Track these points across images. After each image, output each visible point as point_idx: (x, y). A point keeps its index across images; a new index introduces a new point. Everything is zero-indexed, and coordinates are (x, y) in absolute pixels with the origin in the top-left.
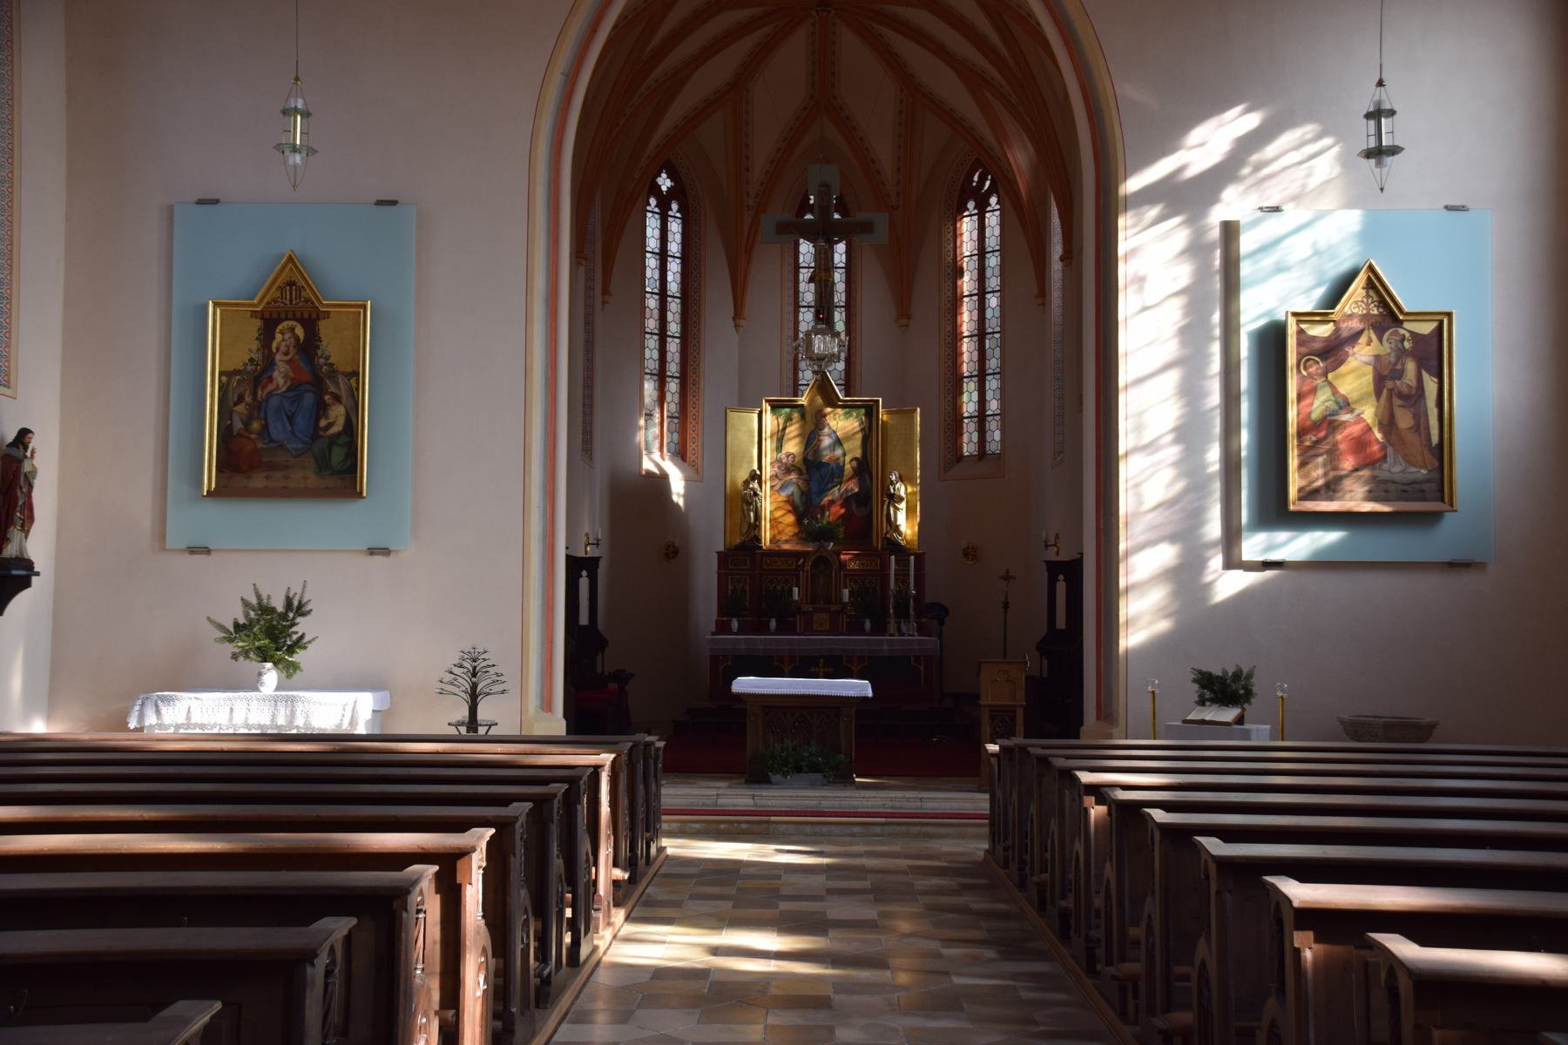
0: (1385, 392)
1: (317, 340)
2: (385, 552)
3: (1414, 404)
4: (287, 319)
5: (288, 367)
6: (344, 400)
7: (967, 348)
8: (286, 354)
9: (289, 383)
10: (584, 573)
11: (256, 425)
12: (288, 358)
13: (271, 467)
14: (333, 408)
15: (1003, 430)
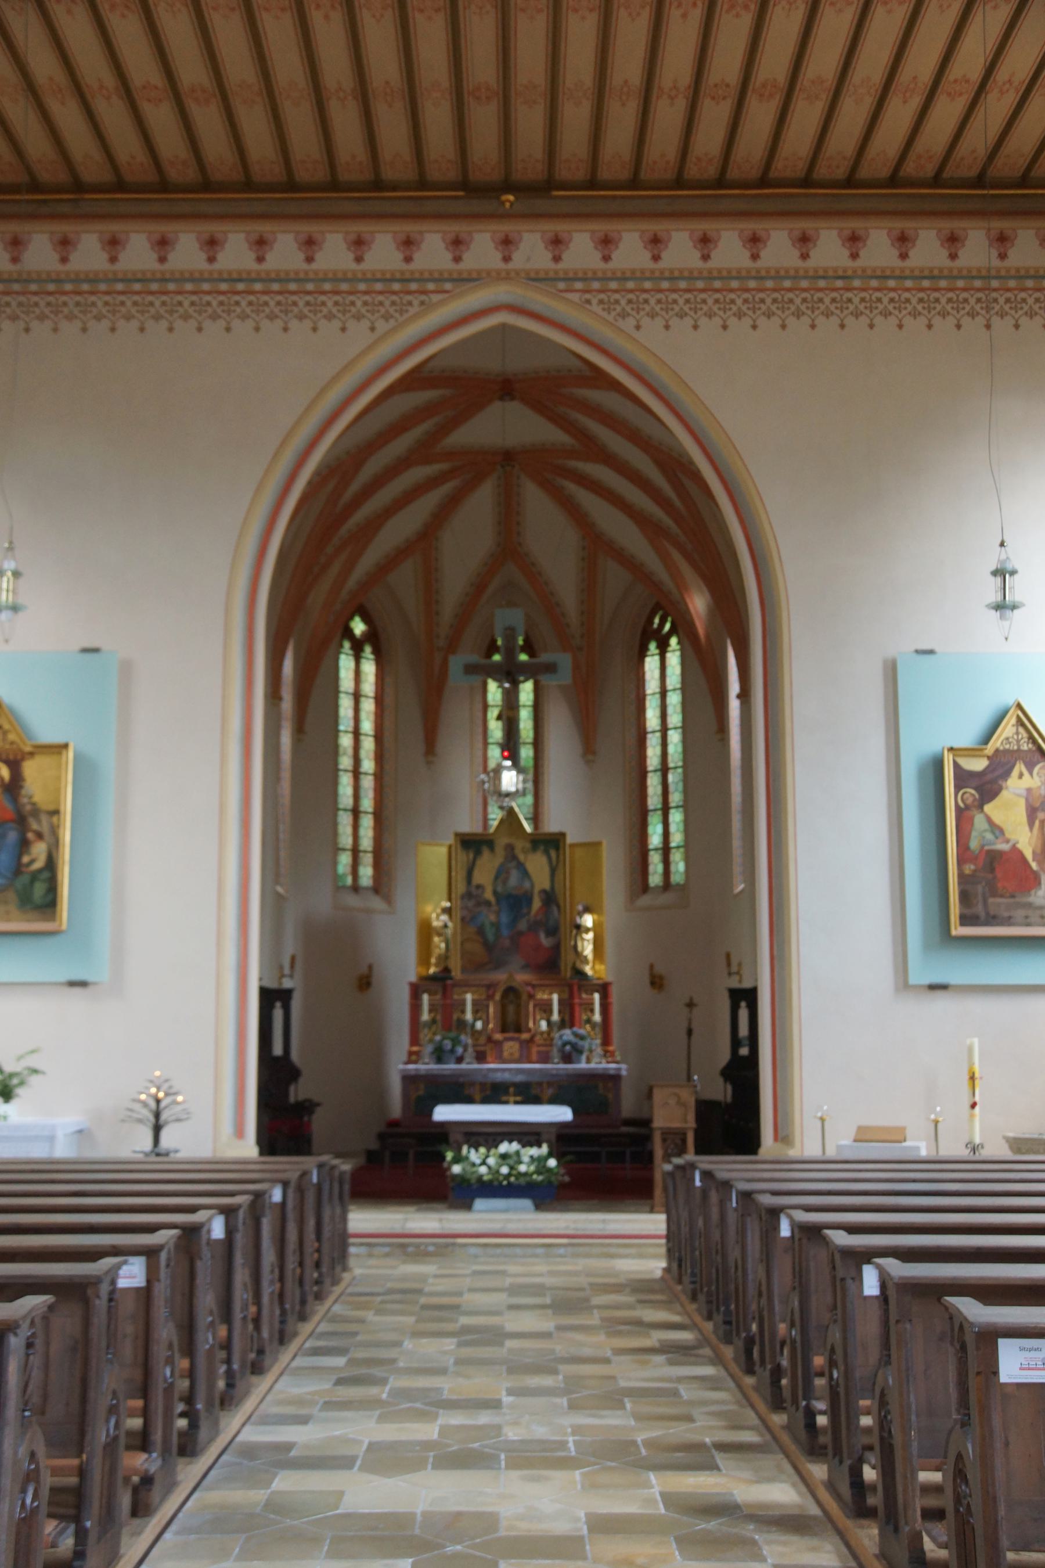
0: (1037, 823)
2: (83, 984)
7: (653, 782)
10: (278, 1004)
15: (687, 860)
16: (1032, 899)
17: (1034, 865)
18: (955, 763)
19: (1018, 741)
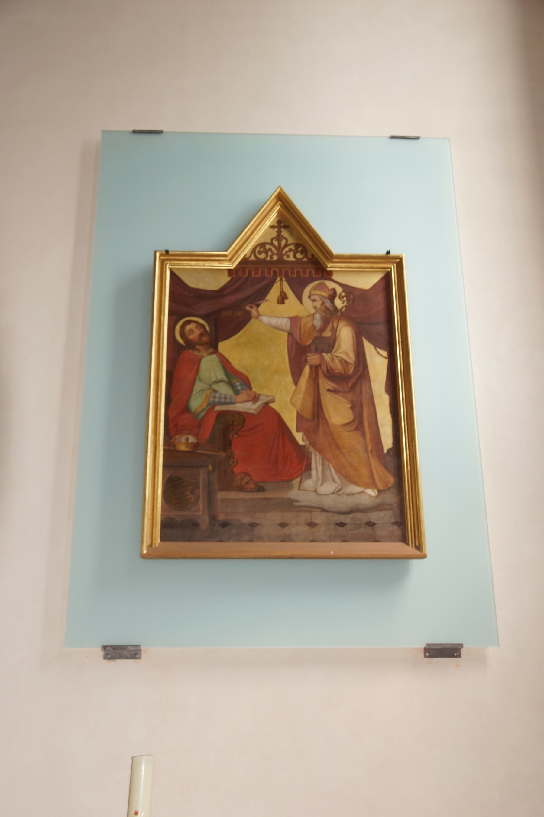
0: (307, 369)
3: (353, 388)
16: (293, 494)
17: (299, 437)
18: (172, 273)
19: (279, 249)
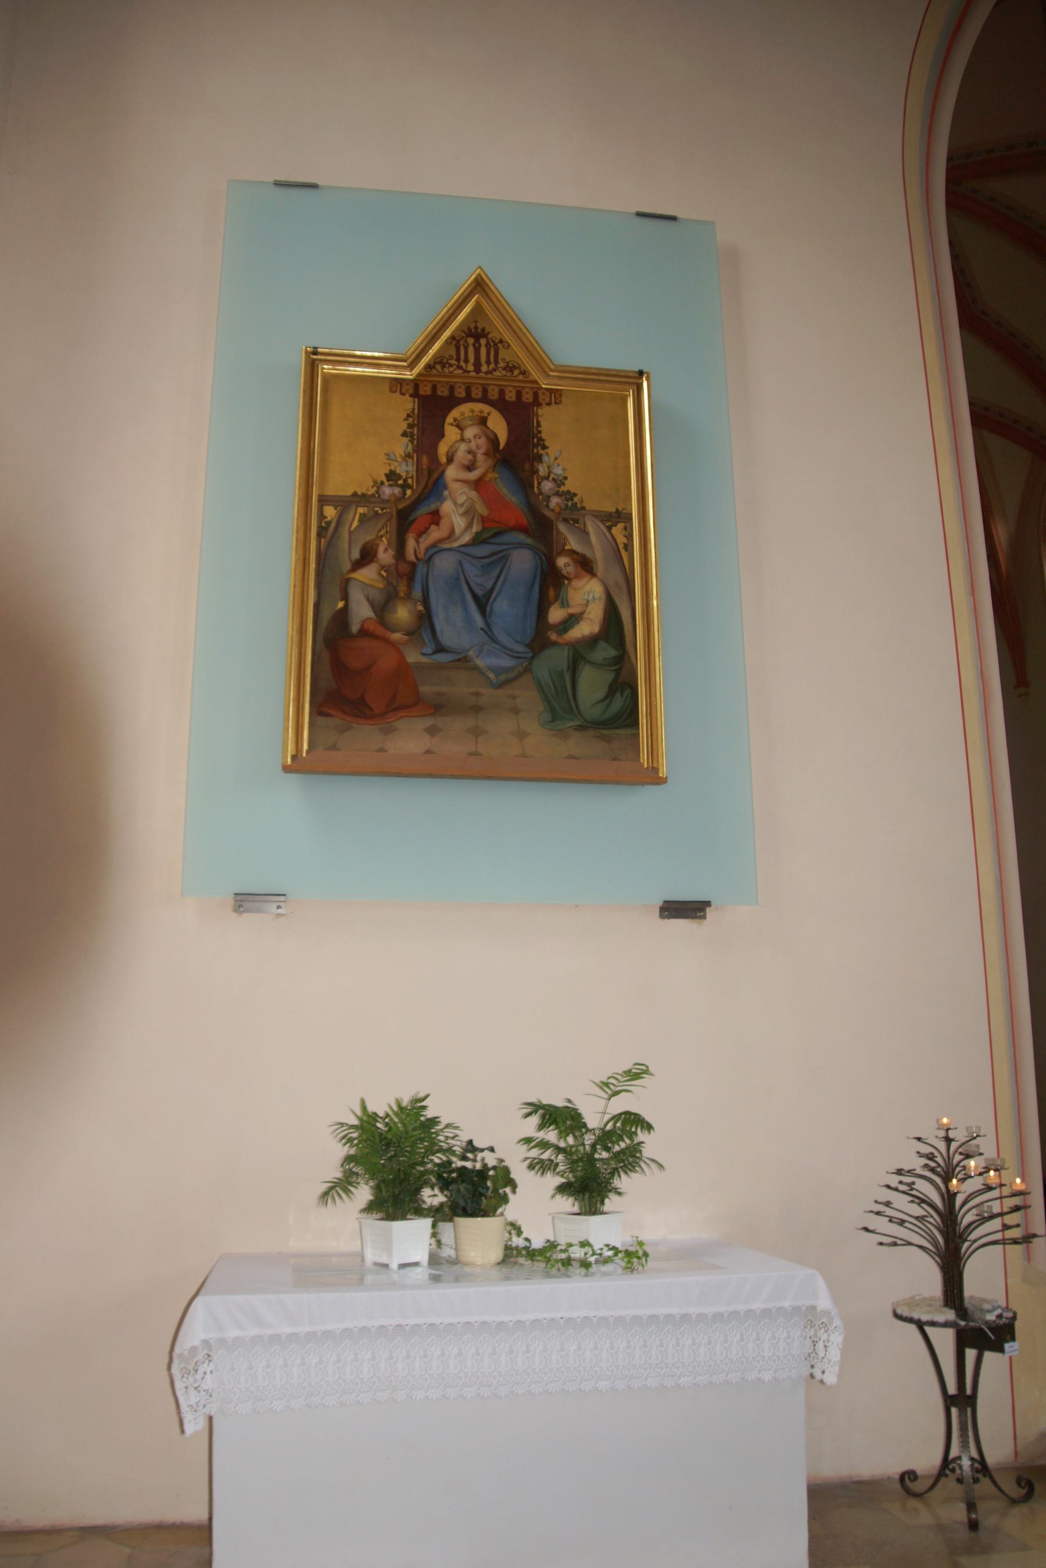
1: (536, 446)
4: (469, 399)
5: (473, 494)
6: (600, 567)
8: (470, 467)
9: (476, 528)
11: (403, 614)
12: (474, 475)
13: (438, 707)
14: (576, 583)
